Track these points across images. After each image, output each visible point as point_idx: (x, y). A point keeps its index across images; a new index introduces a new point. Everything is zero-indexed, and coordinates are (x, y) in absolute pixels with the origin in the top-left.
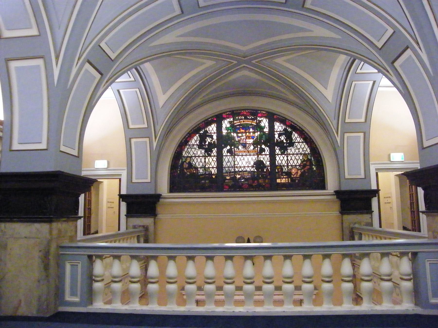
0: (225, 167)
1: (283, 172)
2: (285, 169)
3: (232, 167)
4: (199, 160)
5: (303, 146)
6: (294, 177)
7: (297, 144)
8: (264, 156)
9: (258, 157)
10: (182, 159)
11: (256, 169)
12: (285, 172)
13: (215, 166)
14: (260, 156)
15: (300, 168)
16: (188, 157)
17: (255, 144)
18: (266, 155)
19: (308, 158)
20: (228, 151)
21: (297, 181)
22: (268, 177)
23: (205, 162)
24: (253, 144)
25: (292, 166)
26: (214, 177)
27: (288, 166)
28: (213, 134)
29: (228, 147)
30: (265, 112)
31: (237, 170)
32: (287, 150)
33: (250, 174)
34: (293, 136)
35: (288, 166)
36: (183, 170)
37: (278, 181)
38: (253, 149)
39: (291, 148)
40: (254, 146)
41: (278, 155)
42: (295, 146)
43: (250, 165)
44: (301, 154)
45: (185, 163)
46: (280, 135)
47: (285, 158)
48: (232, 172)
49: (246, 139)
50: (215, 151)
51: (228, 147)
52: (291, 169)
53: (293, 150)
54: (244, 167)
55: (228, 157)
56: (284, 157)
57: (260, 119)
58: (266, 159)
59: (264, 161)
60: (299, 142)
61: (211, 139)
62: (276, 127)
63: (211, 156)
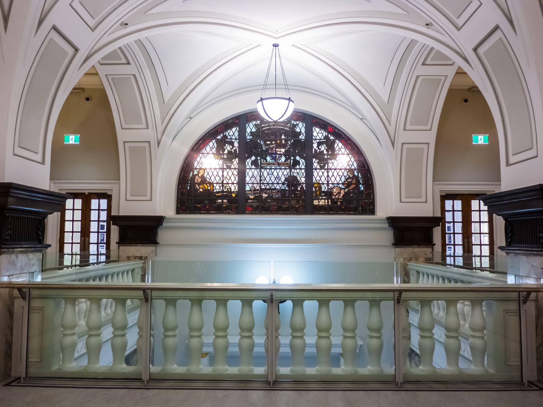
0: (248, 183)
1: (321, 192)
2: (324, 188)
3: (258, 184)
4: (215, 174)
6: (336, 199)
8: (298, 171)
9: (290, 171)
10: (193, 172)
12: (324, 192)
13: (235, 182)
15: (343, 187)
16: (200, 169)
17: (287, 155)
18: (301, 169)
19: (354, 175)
20: (253, 163)
21: (339, 203)
22: (303, 197)
23: (223, 176)
25: (333, 184)
26: (234, 195)
27: (328, 184)
28: (234, 140)
29: (253, 158)
30: (301, 114)
31: (263, 187)
32: (328, 163)
33: (279, 194)
35: (328, 184)
37: (316, 202)
38: (285, 161)
39: (333, 161)
40: (285, 157)
41: (316, 169)
43: (280, 182)
45: (197, 177)
46: (319, 144)
47: (326, 174)
48: (258, 190)
49: (275, 149)
50: (236, 161)
51: (253, 158)
52: (332, 189)
53: (336, 164)
54: (273, 184)
55: (253, 170)
56: (323, 173)
57: (295, 123)
59: (298, 176)
61: (231, 147)
62: (315, 134)
63: (230, 169)
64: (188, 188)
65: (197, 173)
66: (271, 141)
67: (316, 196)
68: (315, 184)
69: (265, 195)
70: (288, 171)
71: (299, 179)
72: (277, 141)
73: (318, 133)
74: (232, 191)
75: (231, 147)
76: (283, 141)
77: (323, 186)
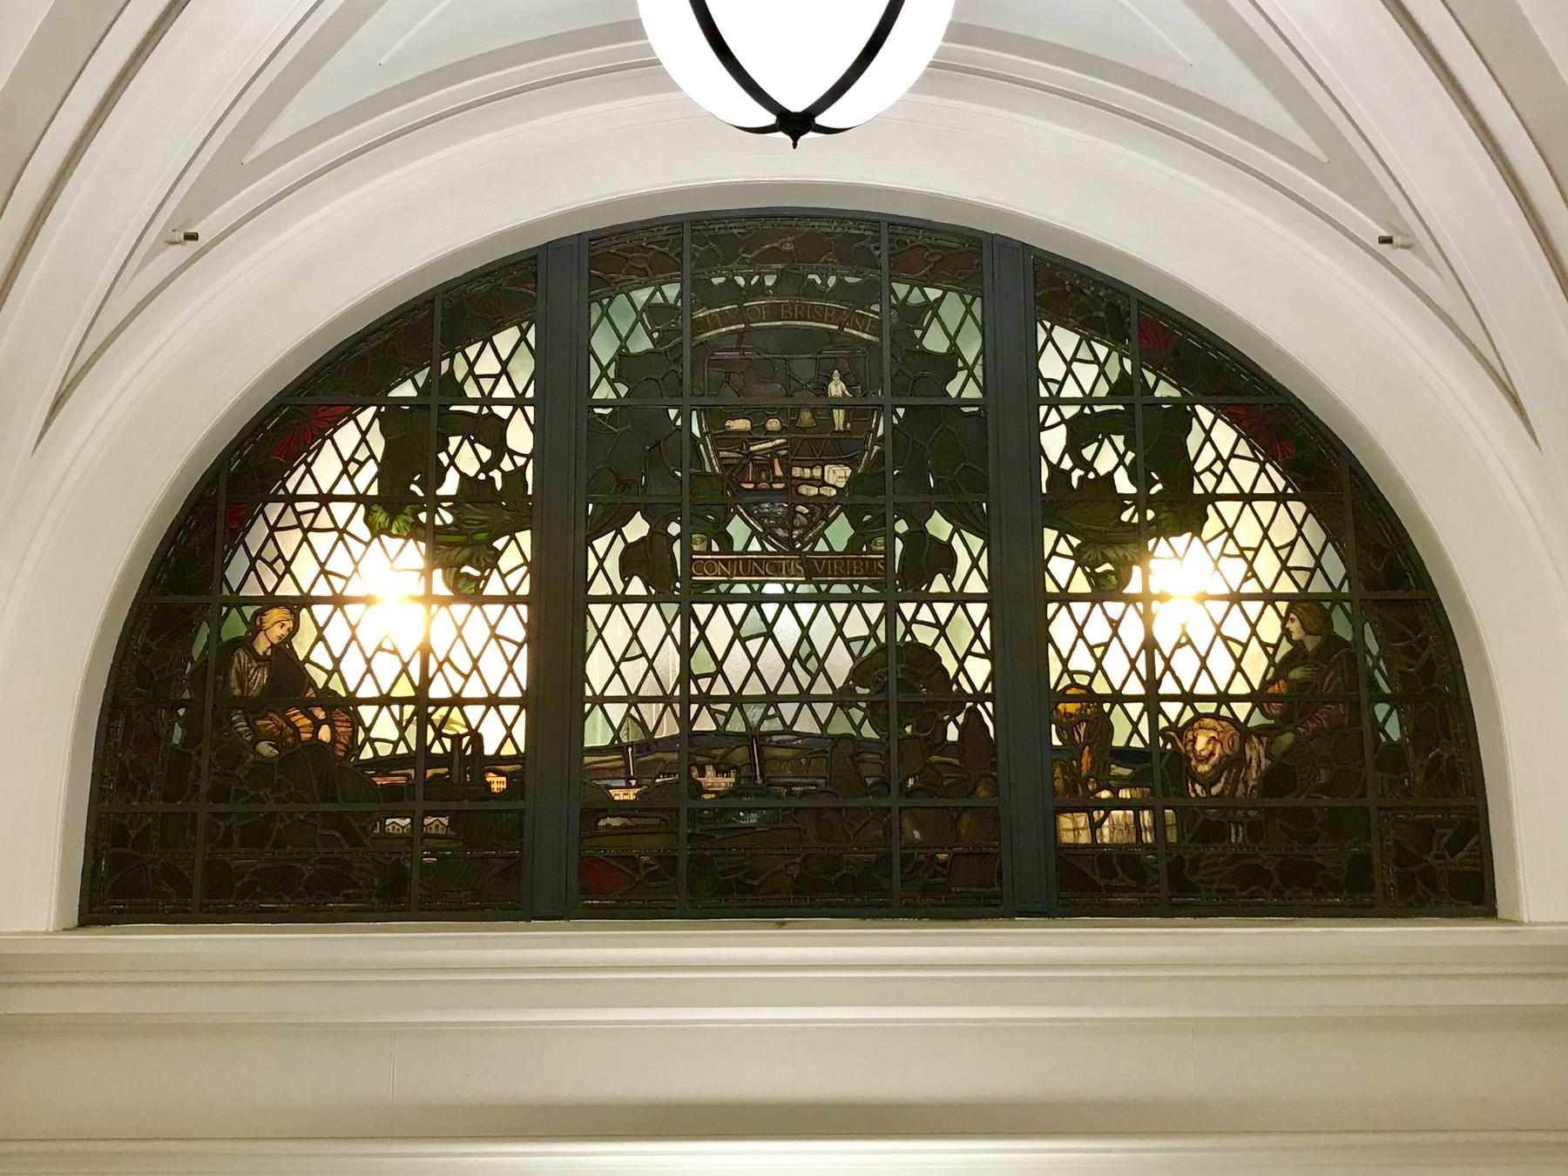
0: (600, 700)
3: (666, 699)
5: (1283, 532)
7: (1229, 509)
8: (943, 609)
9: (890, 614)
11: (872, 714)
13: (511, 690)
14: (908, 609)
15: (1257, 720)
16: (271, 601)
18: (960, 599)
20: (632, 561)
21: (1236, 836)
22: (982, 791)
24: (851, 502)
25: (1188, 698)
26: (497, 783)
27: (1152, 700)
28: (503, 411)
29: (637, 529)
31: (705, 723)
32: (1144, 556)
34: (1194, 440)
35: (1152, 700)
36: (222, 721)
37: (1072, 828)
41: (1065, 598)
42: (1212, 526)
43: (822, 688)
44: (1269, 598)
45: (242, 656)
46: (1082, 432)
50: (515, 552)
51: (637, 529)
52: (1178, 731)
54: (772, 699)
55: (635, 611)
56: (1115, 625)
57: (916, 298)
58: (961, 635)
60: (1247, 498)
61: (486, 455)
62: (1051, 366)
63: (478, 599)
64: (178, 734)
65: (242, 631)
66: (757, 414)
67: (1071, 788)
68: (1063, 696)
69: (714, 781)
70: (874, 610)
71: (951, 666)
72: (797, 411)
73: (1070, 365)
74: (489, 749)
75: (486, 455)
76: (839, 416)
77: (1117, 717)
